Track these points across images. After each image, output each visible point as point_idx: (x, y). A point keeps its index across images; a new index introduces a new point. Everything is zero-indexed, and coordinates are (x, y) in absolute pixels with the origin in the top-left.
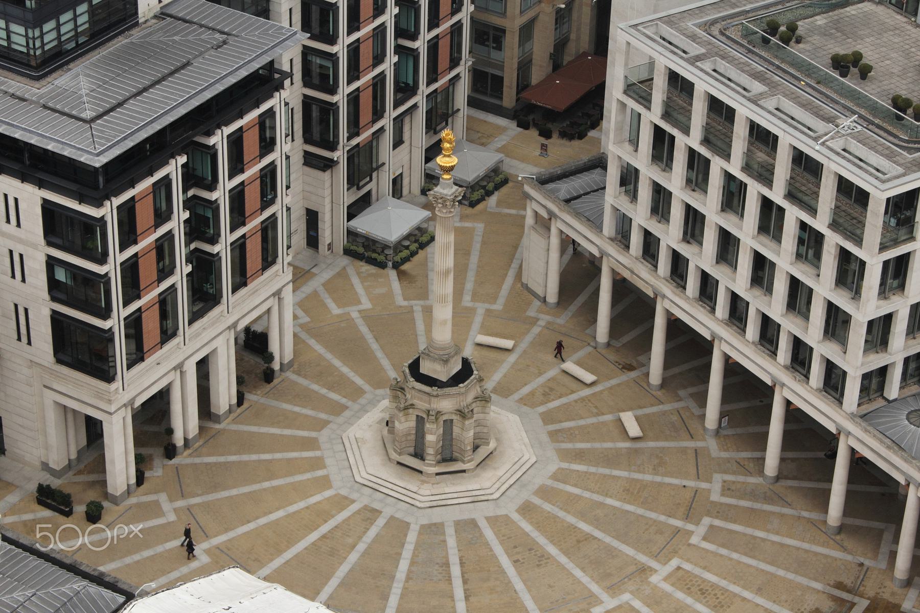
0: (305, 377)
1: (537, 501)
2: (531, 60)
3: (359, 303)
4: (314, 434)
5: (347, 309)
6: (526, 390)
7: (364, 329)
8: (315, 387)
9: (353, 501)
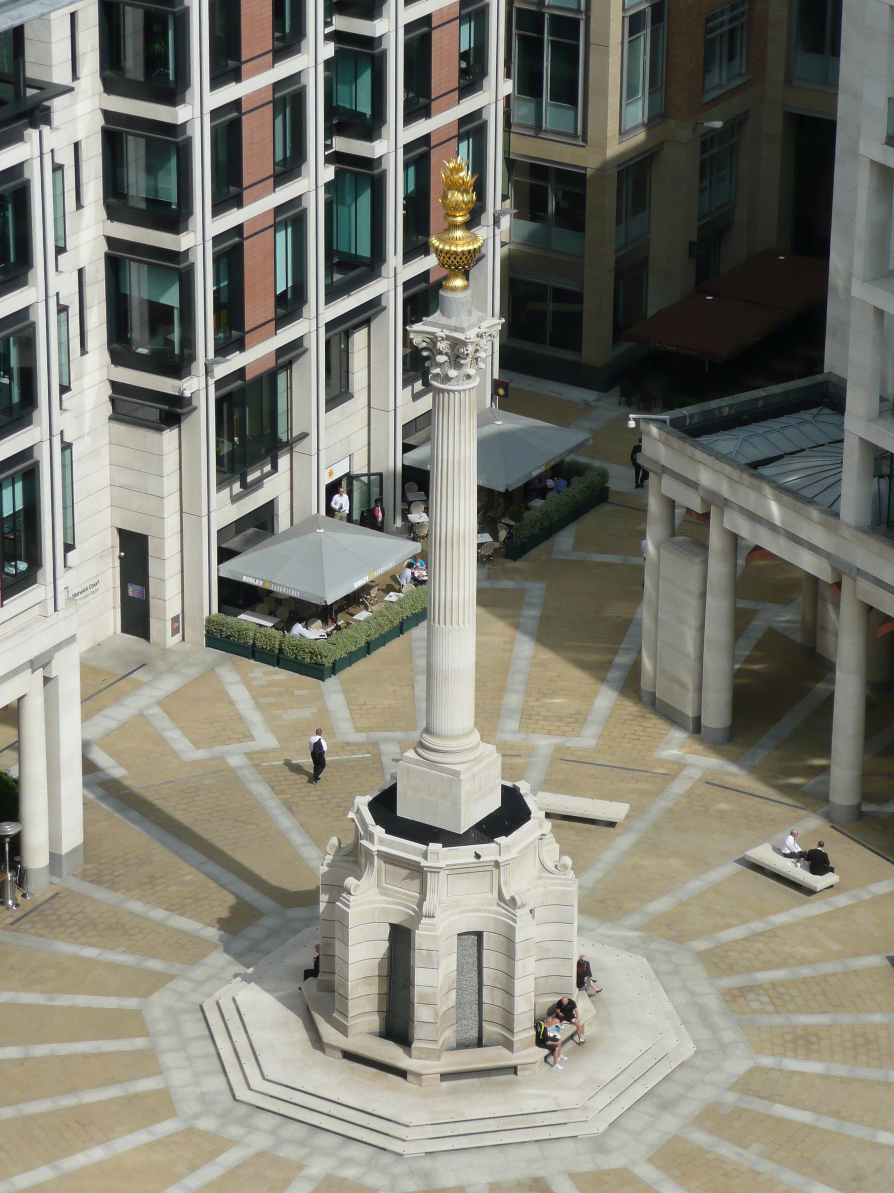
0: (113, 886)
1: (701, 1137)
2: (645, 262)
3: (248, 736)
4: (131, 1003)
5: (219, 750)
6: (660, 905)
7: (260, 790)
8: (137, 906)
9: (234, 1143)
